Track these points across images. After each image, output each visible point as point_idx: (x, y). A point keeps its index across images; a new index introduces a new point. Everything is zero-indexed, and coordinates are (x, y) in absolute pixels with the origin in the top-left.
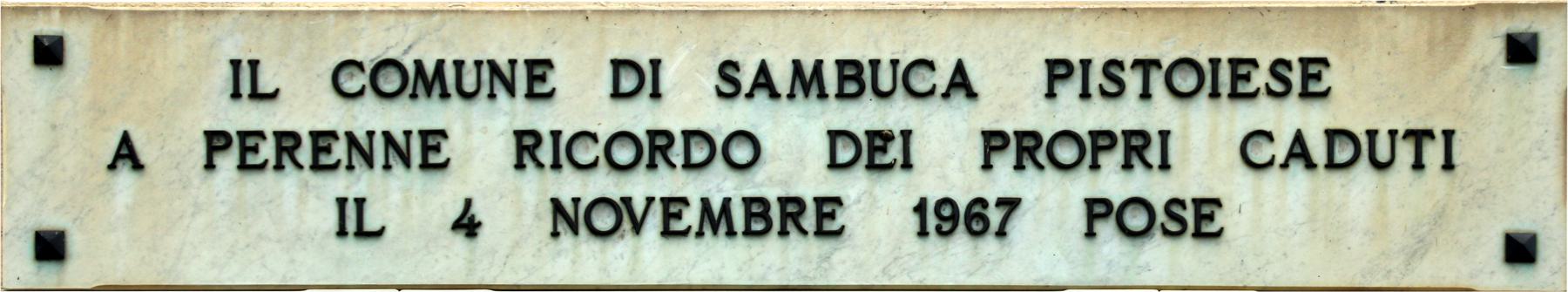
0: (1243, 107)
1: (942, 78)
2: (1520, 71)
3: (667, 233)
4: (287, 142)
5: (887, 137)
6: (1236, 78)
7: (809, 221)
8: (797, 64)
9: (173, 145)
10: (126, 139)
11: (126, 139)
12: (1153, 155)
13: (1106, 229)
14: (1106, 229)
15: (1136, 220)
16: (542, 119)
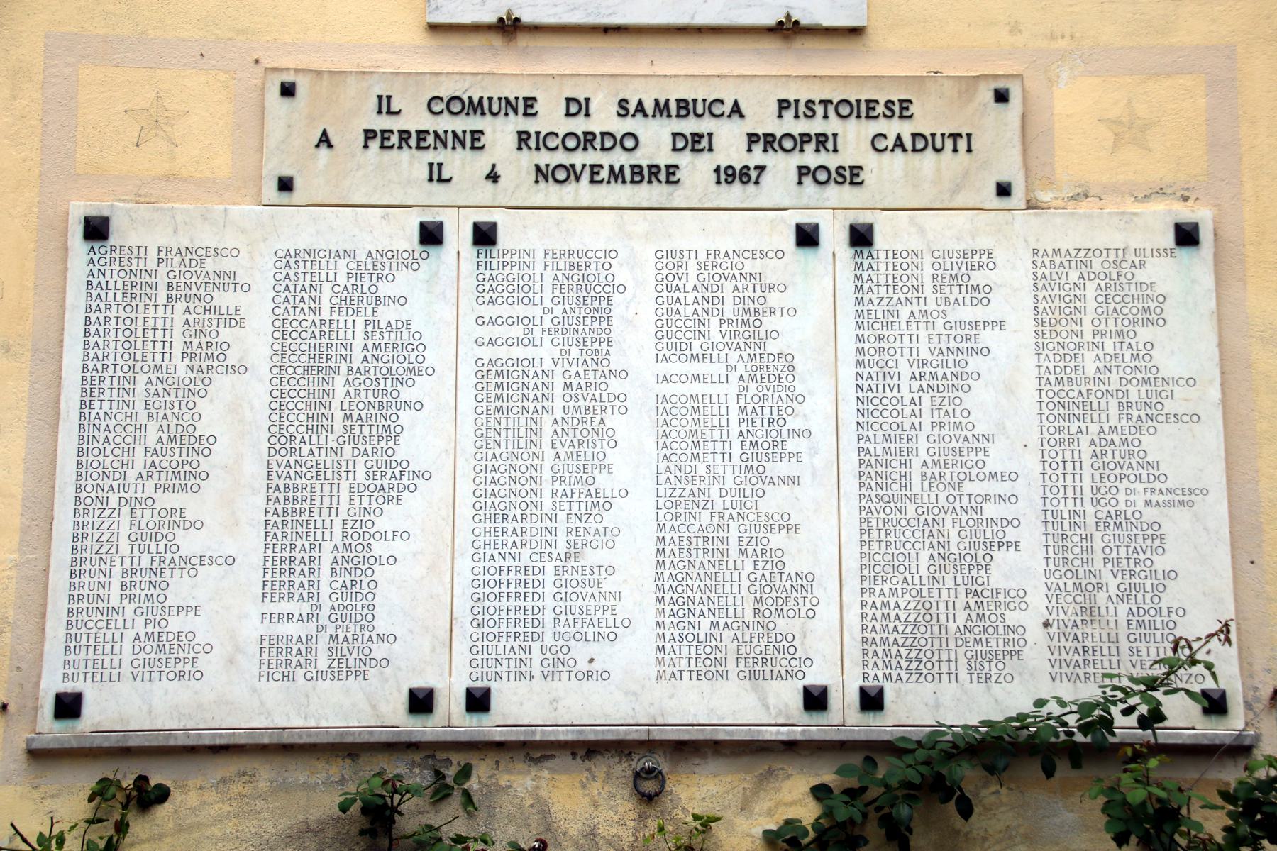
0: (872, 123)
1: (727, 108)
2: (1001, 106)
3: (592, 181)
4: (404, 135)
5: (701, 136)
6: (868, 109)
7: (662, 176)
8: (657, 101)
9: (348, 136)
10: (324, 133)
11: (324, 133)
12: (830, 145)
13: (808, 180)
14: (808, 180)
15: (822, 176)
16: (531, 126)
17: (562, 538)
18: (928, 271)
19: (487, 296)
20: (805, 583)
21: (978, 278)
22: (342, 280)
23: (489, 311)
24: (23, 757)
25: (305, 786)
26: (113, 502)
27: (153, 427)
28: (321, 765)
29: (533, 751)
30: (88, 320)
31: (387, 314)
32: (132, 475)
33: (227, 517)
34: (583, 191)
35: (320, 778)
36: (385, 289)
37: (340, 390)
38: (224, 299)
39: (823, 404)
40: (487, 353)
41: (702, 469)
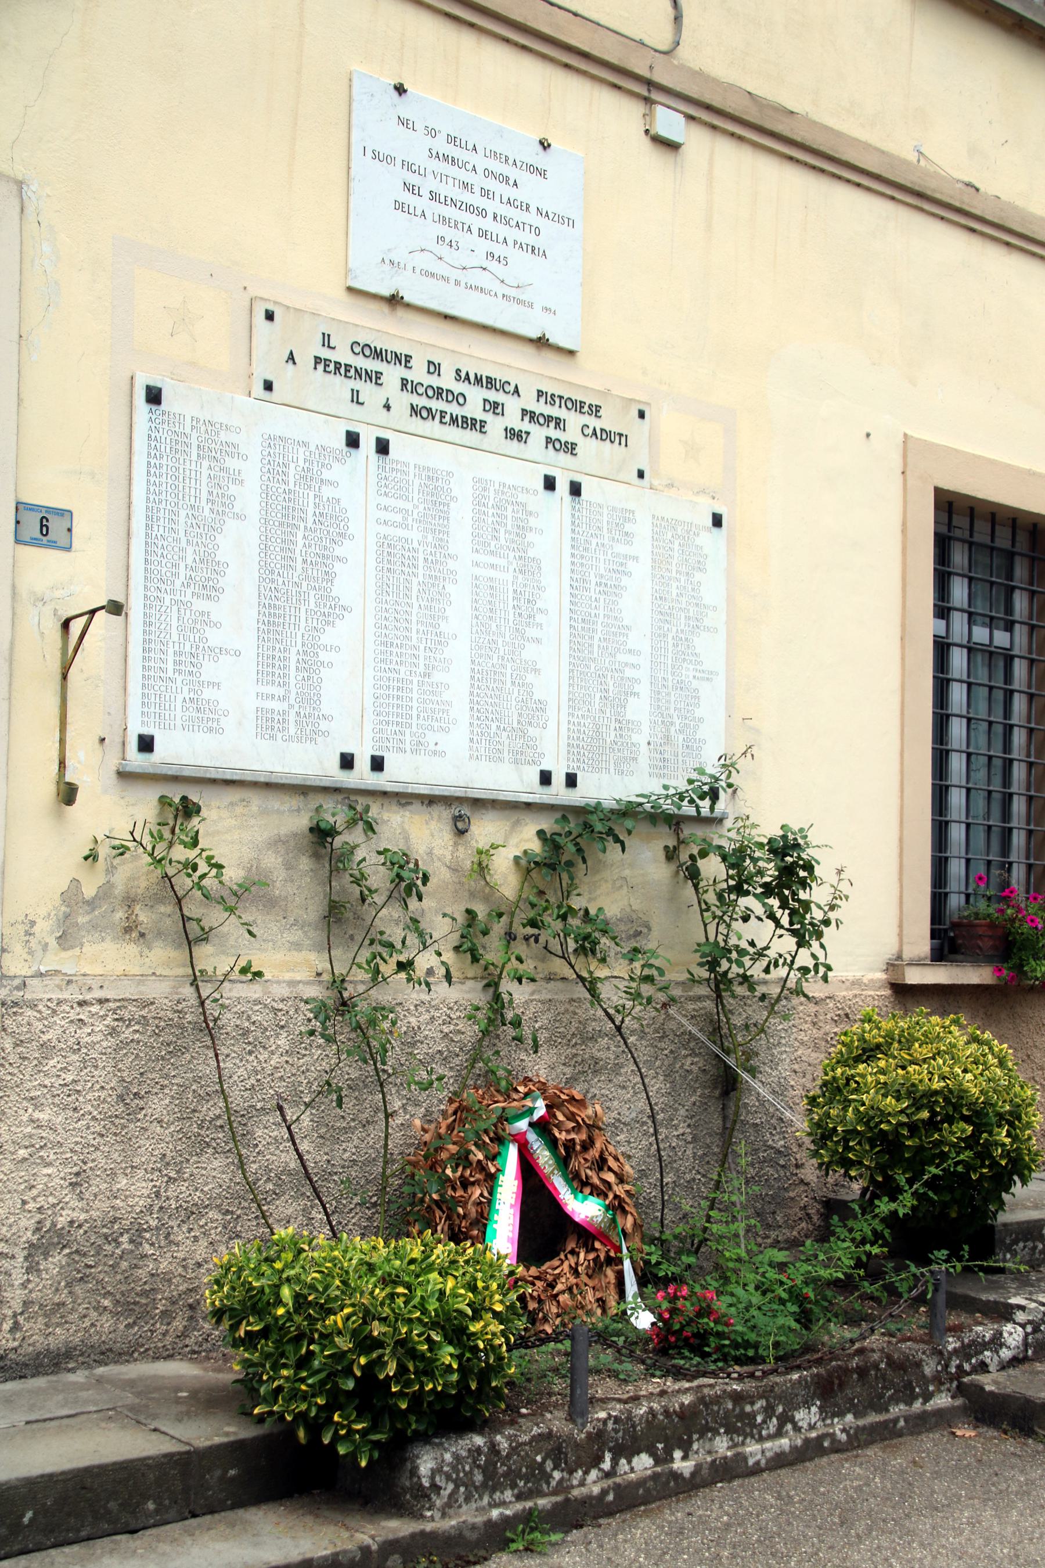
1: (512, 388)
9: (305, 360)
10: (291, 353)
11: (291, 353)
13: (550, 446)
16: (409, 375)
17: (422, 662)
18: (605, 519)
19: (383, 490)
20: (541, 706)
21: (628, 527)
22: (301, 463)
23: (385, 501)
24: (114, 776)
25: (278, 811)
26: (167, 602)
27: (190, 550)
28: (287, 798)
29: (402, 799)
30: (149, 463)
31: (327, 492)
32: (178, 583)
33: (234, 620)
34: (433, 427)
35: (285, 807)
36: (326, 475)
37: (300, 543)
38: (232, 463)
39: (553, 594)
40: (384, 530)
41: (494, 628)
